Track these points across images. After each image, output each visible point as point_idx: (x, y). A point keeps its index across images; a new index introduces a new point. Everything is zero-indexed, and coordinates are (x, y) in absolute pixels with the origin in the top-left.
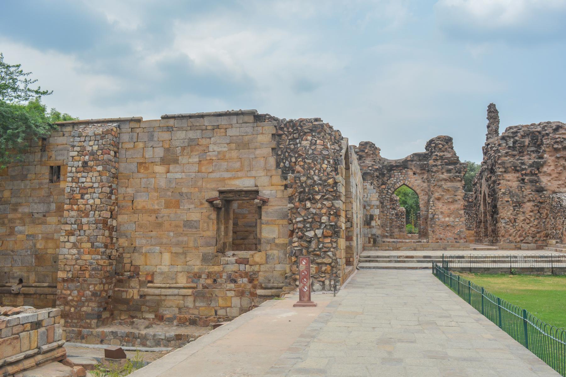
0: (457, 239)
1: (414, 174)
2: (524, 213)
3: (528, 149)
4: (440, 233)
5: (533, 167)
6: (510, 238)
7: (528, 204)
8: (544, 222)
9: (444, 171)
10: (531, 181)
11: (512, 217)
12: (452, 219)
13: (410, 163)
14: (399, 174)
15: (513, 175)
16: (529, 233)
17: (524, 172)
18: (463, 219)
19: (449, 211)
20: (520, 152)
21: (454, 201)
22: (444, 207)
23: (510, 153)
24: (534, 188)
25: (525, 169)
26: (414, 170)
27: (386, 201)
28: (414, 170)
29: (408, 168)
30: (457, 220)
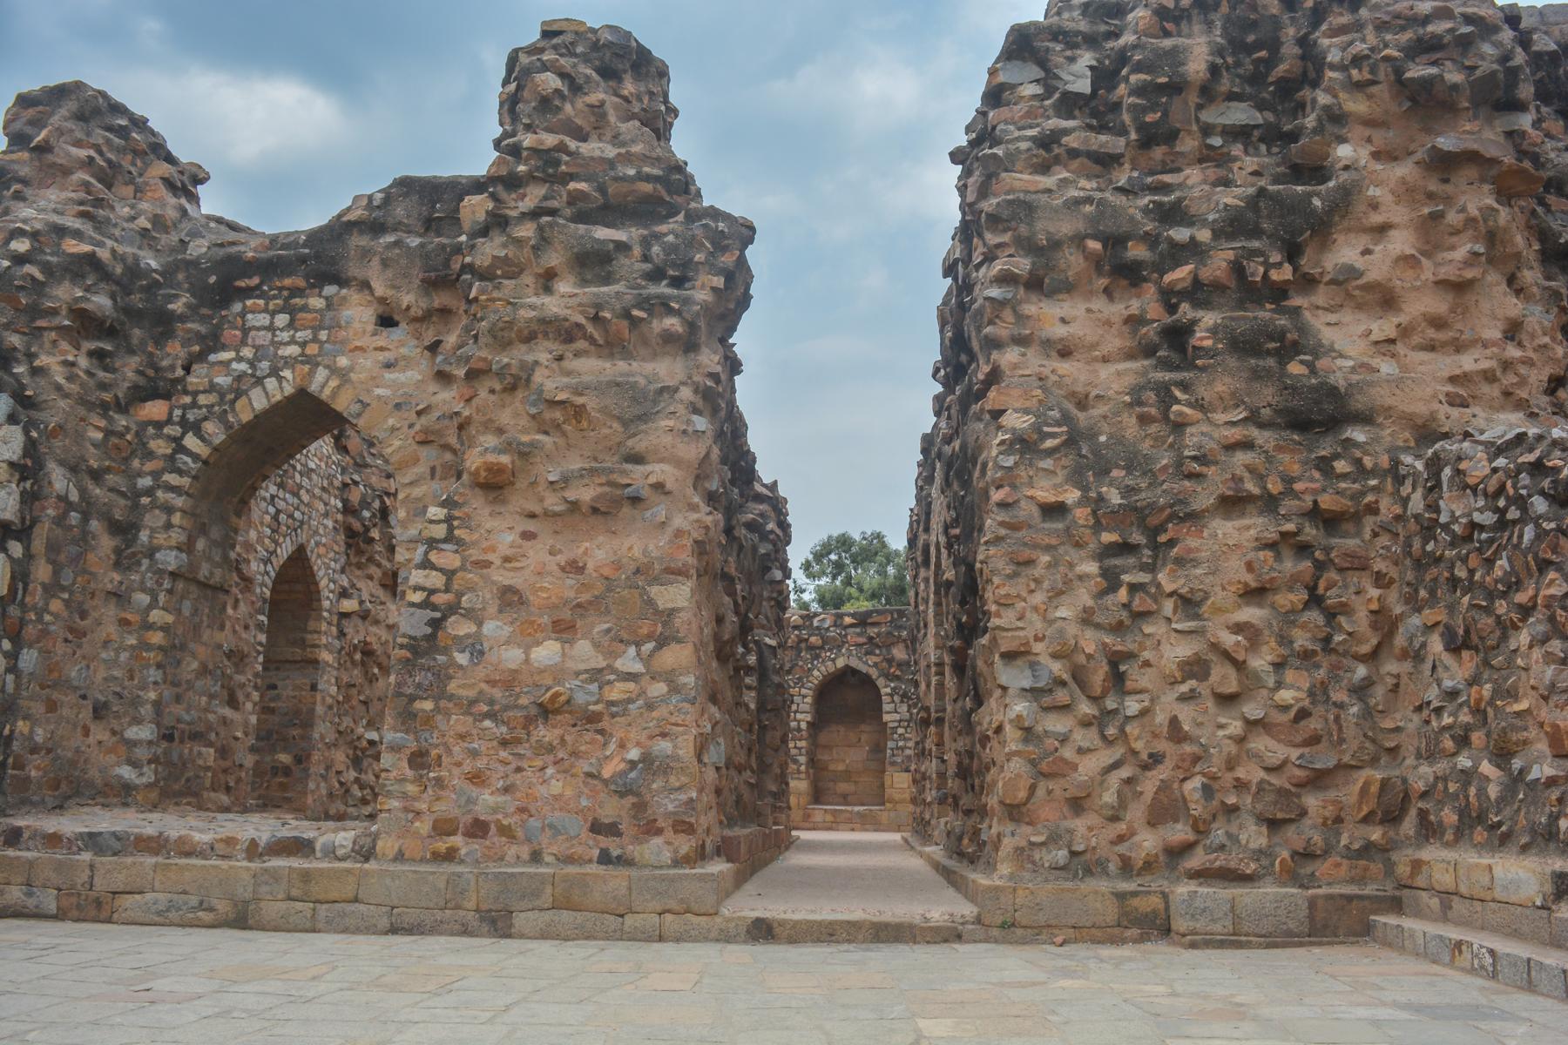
0: (612, 830)
1: (386, 321)
2: (1189, 604)
3: (1208, 116)
4: (476, 778)
5: (1256, 233)
6: (1080, 825)
7: (1226, 529)
8: (1361, 690)
9: (554, 258)
10: (1244, 345)
11: (1090, 641)
12: (585, 653)
13: (358, 241)
14: (282, 319)
15: (1099, 303)
16: (1240, 785)
17: (1180, 275)
18: (677, 656)
19: (568, 587)
20: (1149, 138)
21: (615, 505)
22: (537, 554)
23: (1071, 141)
24: (1267, 395)
25: (1193, 249)
26: (380, 289)
27: (155, 519)
28: (380, 289)
29: (342, 282)
30: (629, 661)
